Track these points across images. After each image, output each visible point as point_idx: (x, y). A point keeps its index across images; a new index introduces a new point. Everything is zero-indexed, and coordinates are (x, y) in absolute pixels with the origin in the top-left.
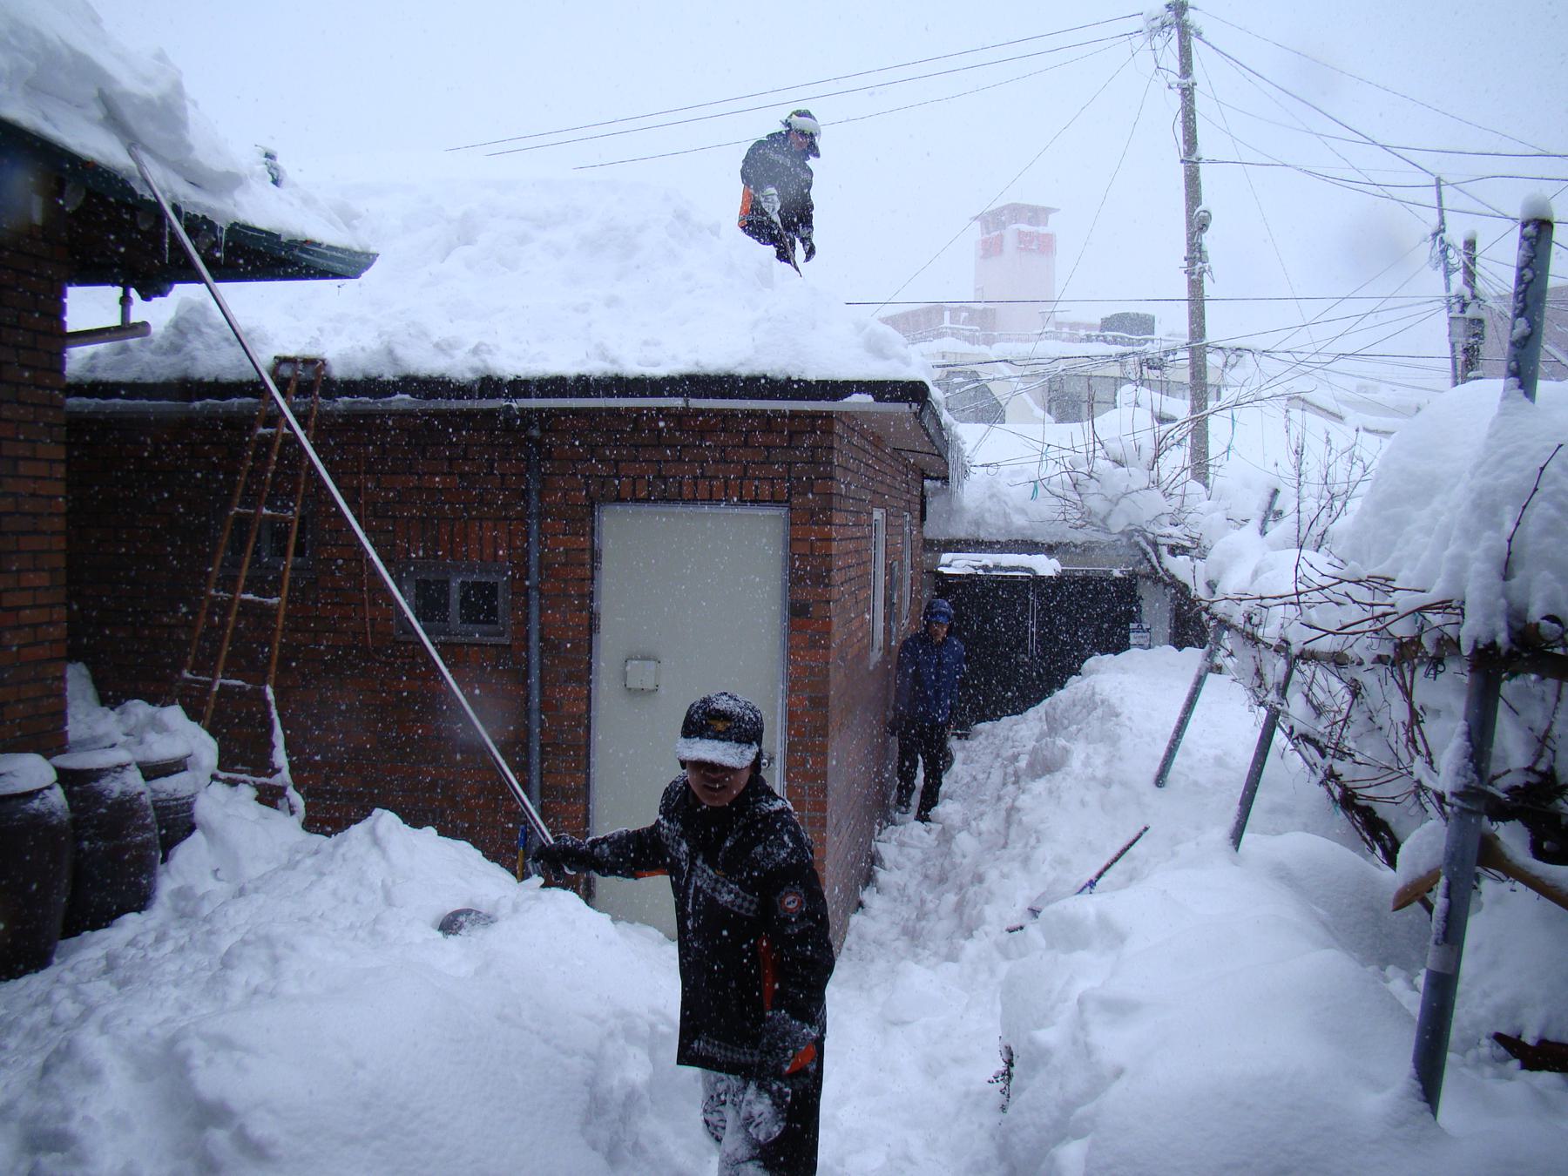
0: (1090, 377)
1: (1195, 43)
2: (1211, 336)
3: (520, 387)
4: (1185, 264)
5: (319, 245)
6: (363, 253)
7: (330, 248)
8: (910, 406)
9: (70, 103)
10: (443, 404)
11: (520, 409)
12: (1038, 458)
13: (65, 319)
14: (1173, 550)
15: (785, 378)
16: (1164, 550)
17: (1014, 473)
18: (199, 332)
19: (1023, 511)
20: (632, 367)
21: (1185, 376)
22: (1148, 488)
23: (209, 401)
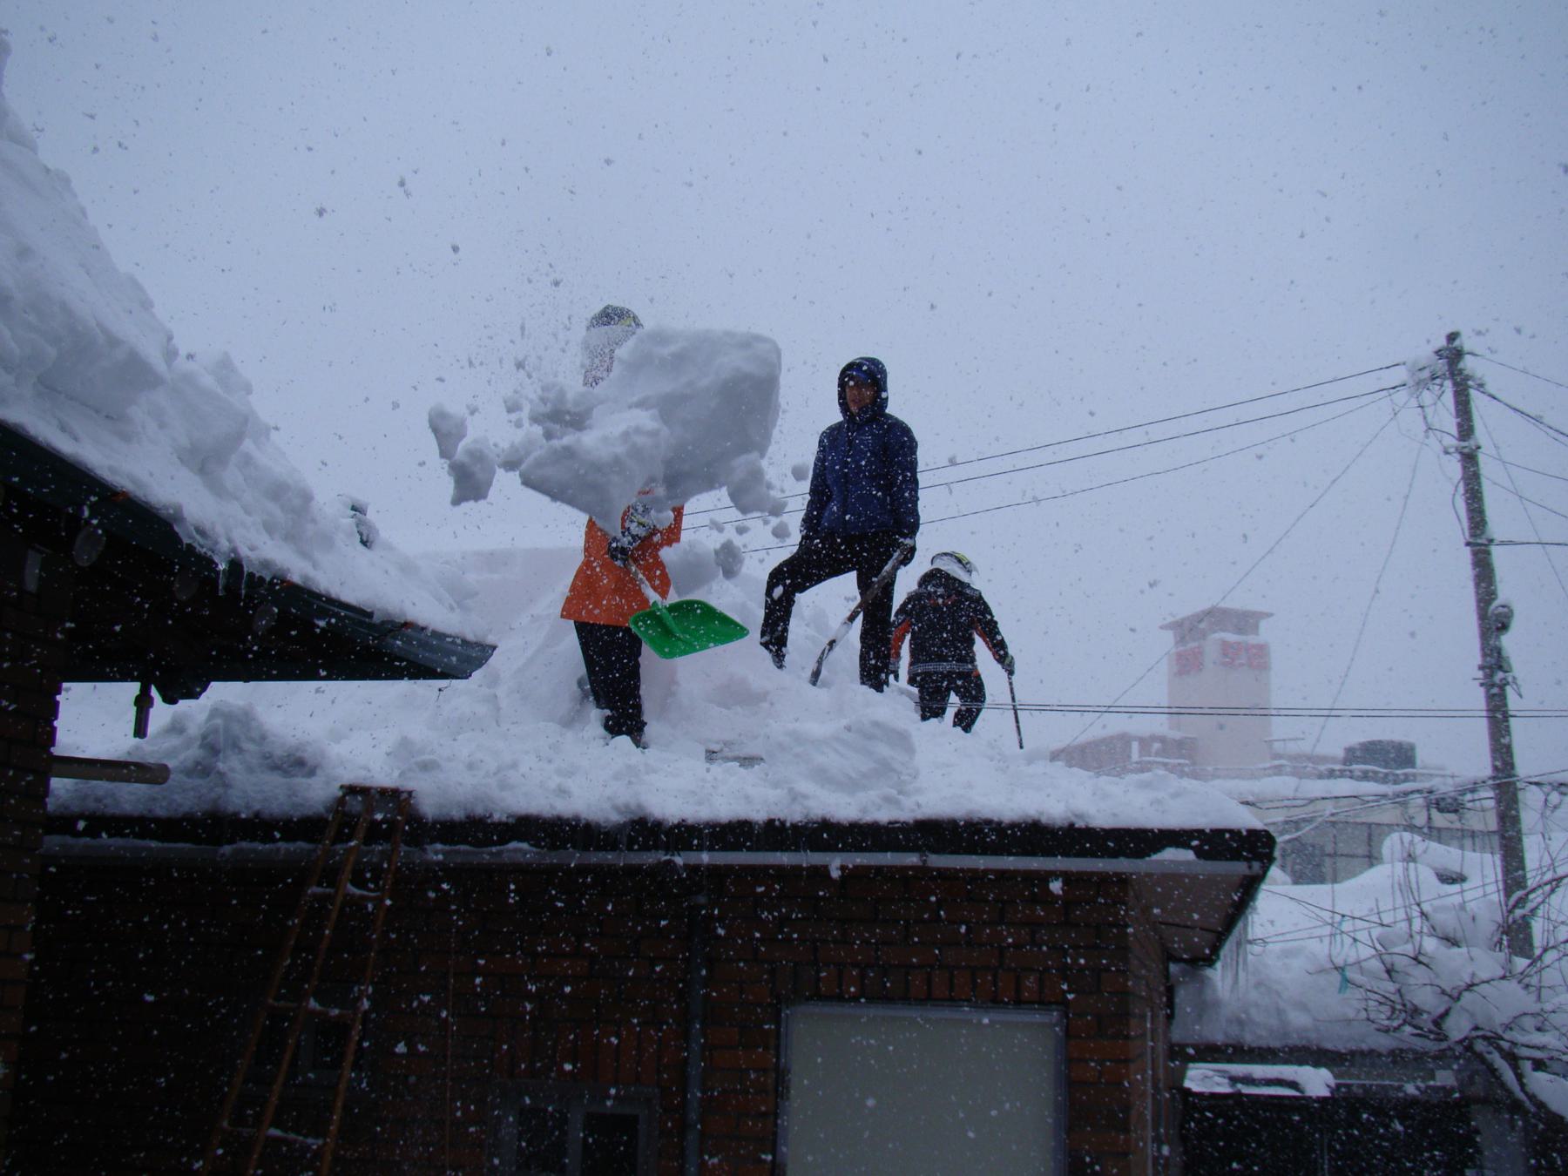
0: (1369, 825)
1: (1477, 400)
2: (1524, 766)
3: (685, 835)
4: (1480, 674)
5: (423, 629)
6: (478, 644)
7: (436, 634)
8: (1250, 867)
9: (97, 412)
10: (575, 858)
11: (686, 866)
12: (1327, 930)
13: (56, 723)
14: (1539, 1065)
15: (1066, 824)
16: (1527, 1066)
17: (1287, 954)
18: (236, 746)
19: (1302, 1006)
20: (844, 808)
21: (1493, 824)
22: (1504, 978)
23: (244, 845)
